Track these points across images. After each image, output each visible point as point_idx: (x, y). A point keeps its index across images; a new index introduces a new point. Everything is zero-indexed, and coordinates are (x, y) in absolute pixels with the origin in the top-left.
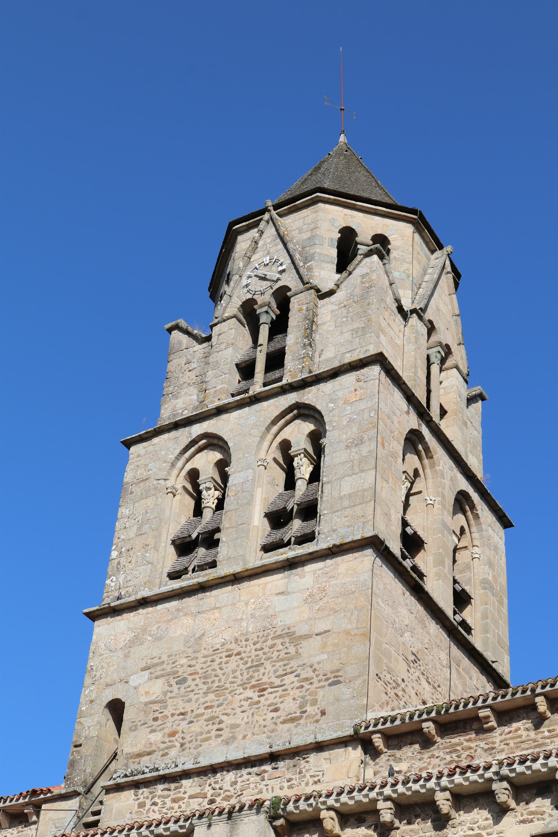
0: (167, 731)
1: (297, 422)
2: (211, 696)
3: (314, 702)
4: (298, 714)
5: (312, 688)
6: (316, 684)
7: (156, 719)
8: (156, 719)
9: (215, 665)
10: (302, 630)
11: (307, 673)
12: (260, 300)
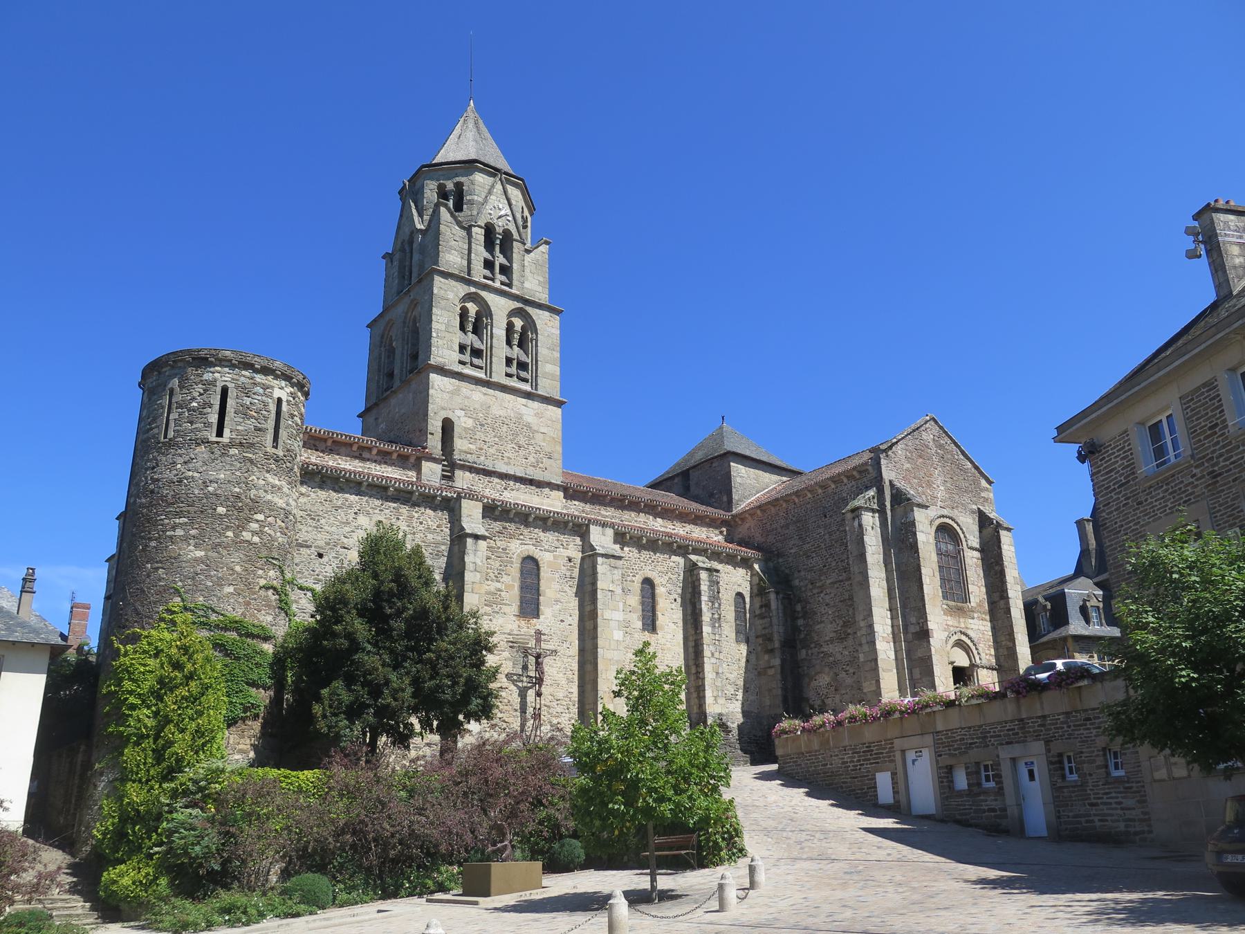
2: (496, 439)
3: (542, 463)
5: (541, 455)
6: (541, 455)
7: (471, 438)
8: (471, 438)
9: (497, 425)
10: (535, 428)
12: (497, 228)
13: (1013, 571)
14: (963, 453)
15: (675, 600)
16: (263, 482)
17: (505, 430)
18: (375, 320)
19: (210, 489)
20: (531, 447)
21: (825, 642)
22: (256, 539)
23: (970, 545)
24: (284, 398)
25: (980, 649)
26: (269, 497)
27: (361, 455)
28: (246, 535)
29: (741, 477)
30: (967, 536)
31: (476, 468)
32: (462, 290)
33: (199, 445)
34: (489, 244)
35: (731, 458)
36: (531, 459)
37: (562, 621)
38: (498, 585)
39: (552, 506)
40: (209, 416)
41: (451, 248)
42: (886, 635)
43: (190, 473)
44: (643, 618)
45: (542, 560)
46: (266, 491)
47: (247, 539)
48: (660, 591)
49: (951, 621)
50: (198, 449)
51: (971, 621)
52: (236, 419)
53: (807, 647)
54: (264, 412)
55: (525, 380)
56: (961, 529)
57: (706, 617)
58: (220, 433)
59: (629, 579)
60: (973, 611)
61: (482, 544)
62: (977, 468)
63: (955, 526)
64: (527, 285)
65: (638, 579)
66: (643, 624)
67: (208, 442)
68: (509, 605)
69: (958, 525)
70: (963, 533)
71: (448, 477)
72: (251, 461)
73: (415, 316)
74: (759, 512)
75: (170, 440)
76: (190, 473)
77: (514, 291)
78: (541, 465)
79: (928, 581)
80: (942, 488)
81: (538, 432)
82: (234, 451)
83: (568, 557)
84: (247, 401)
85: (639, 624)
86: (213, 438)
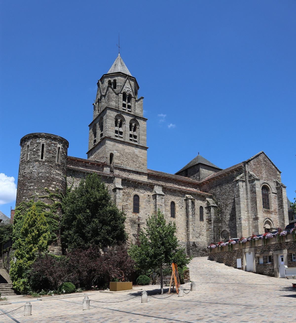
0: (121, 162)
1: (134, 121)
2: (127, 159)
3: (141, 166)
4: (139, 167)
5: (141, 164)
6: (141, 164)
7: (119, 159)
8: (119, 159)
9: (127, 155)
11: (139, 162)
13: (285, 200)
15: (181, 208)
16: (55, 173)
17: (129, 157)
18: (91, 124)
19: (40, 175)
20: (137, 162)
21: (227, 221)
22: (54, 189)
24: (61, 147)
25: (274, 223)
26: (57, 177)
27: (85, 164)
28: (51, 188)
29: (203, 171)
30: (272, 189)
31: (120, 168)
32: (115, 114)
33: (36, 162)
34: (124, 99)
35: (200, 165)
36: (138, 165)
37: (146, 214)
38: (127, 203)
39: (144, 180)
40: (39, 153)
41: (113, 100)
43: (34, 170)
44: (171, 214)
45: (140, 196)
46: (56, 175)
47: (51, 189)
48: (177, 205)
49: (265, 215)
50: (36, 163)
52: (47, 154)
53: (221, 223)
54: (55, 152)
55: (136, 141)
56: (270, 187)
57: (190, 213)
58: (42, 158)
59: (167, 201)
60: (272, 212)
61: (121, 191)
62: (276, 168)
63: (268, 186)
64: (136, 111)
65: (170, 202)
66: (171, 215)
67: (39, 161)
68: (130, 209)
69: (269, 186)
70: (271, 188)
71: (112, 171)
72: (51, 166)
73: (102, 122)
74: (208, 182)
75: (28, 160)
76: (34, 170)
77: (132, 113)
78: (140, 167)
79: (258, 202)
80: (265, 174)
81: (140, 157)
82: (46, 163)
83: (148, 195)
84: (50, 148)
85: (170, 215)
86: (40, 160)
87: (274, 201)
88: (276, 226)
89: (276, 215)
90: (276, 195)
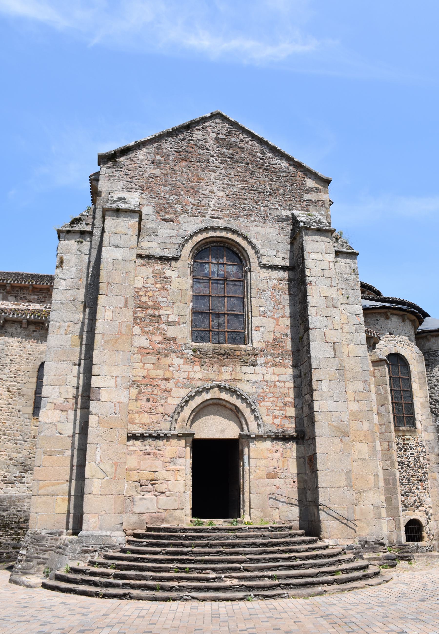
14: (274, 150)
23: (265, 261)
30: (262, 251)
42: (62, 401)
51: (245, 369)
56: (250, 243)
60: (255, 355)
62: (298, 165)
69: (245, 238)
70: (254, 248)
80: (222, 194)
87: (272, 304)
88: (277, 421)
89: (281, 365)
90: (286, 275)
